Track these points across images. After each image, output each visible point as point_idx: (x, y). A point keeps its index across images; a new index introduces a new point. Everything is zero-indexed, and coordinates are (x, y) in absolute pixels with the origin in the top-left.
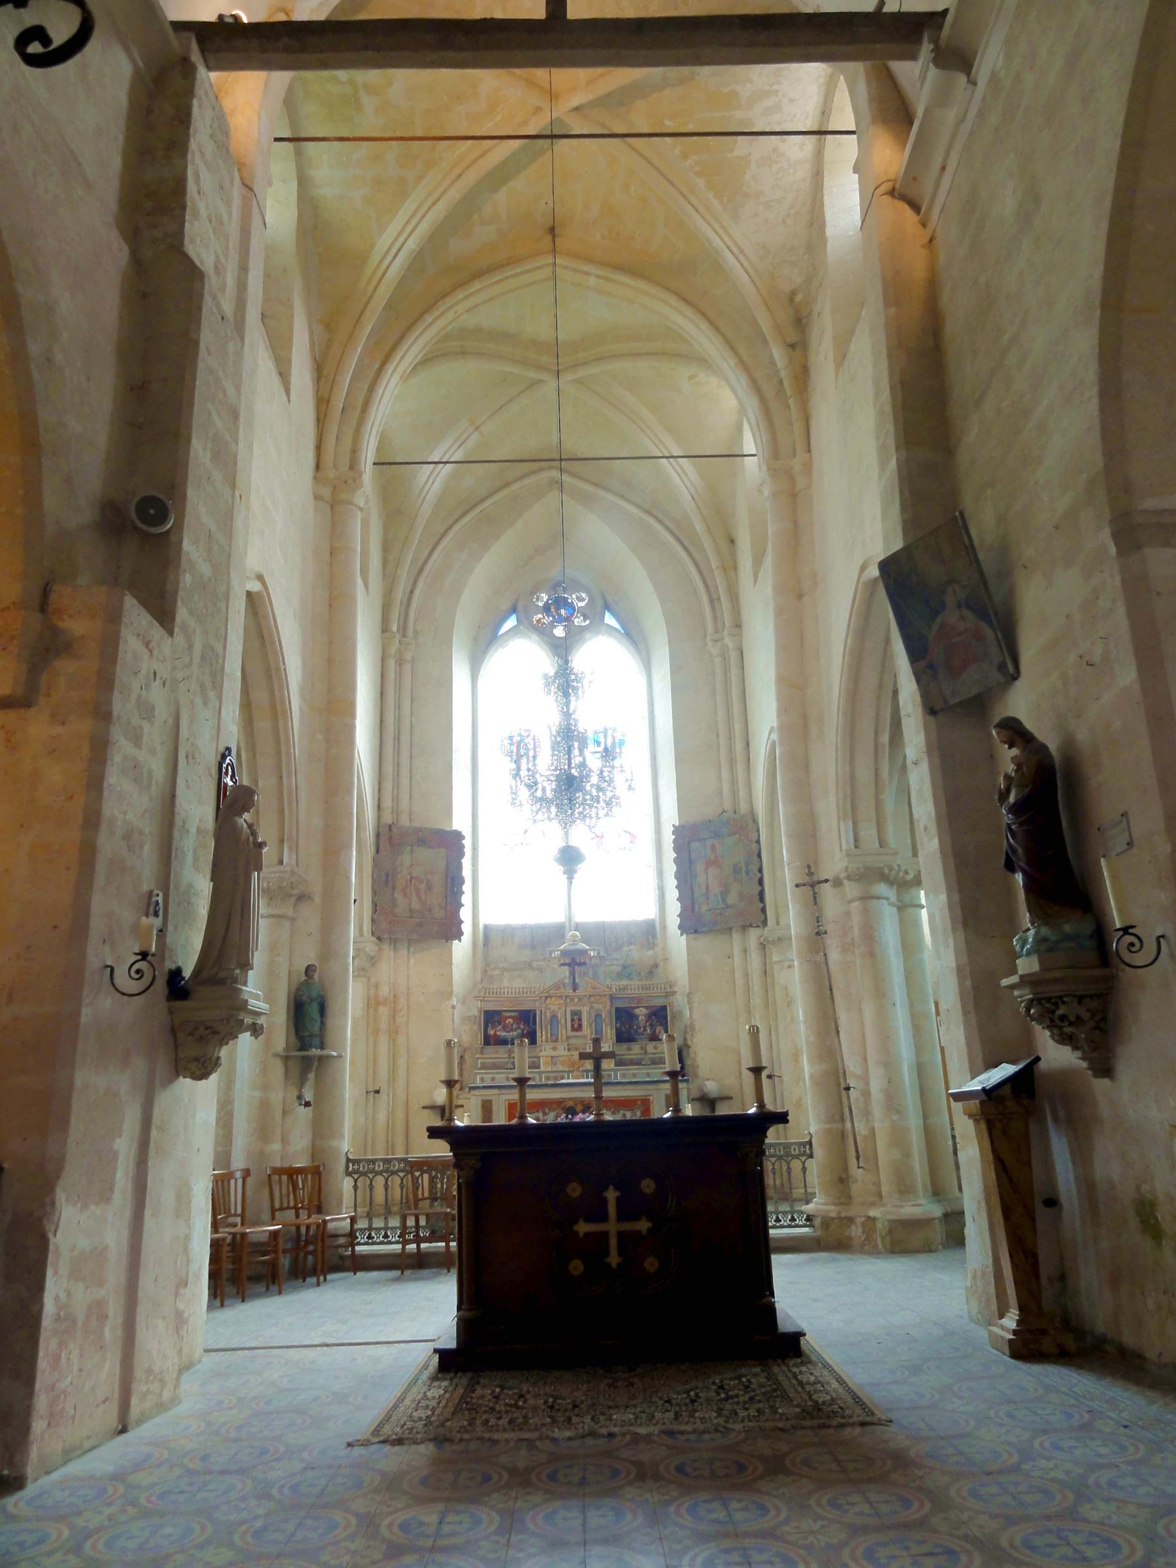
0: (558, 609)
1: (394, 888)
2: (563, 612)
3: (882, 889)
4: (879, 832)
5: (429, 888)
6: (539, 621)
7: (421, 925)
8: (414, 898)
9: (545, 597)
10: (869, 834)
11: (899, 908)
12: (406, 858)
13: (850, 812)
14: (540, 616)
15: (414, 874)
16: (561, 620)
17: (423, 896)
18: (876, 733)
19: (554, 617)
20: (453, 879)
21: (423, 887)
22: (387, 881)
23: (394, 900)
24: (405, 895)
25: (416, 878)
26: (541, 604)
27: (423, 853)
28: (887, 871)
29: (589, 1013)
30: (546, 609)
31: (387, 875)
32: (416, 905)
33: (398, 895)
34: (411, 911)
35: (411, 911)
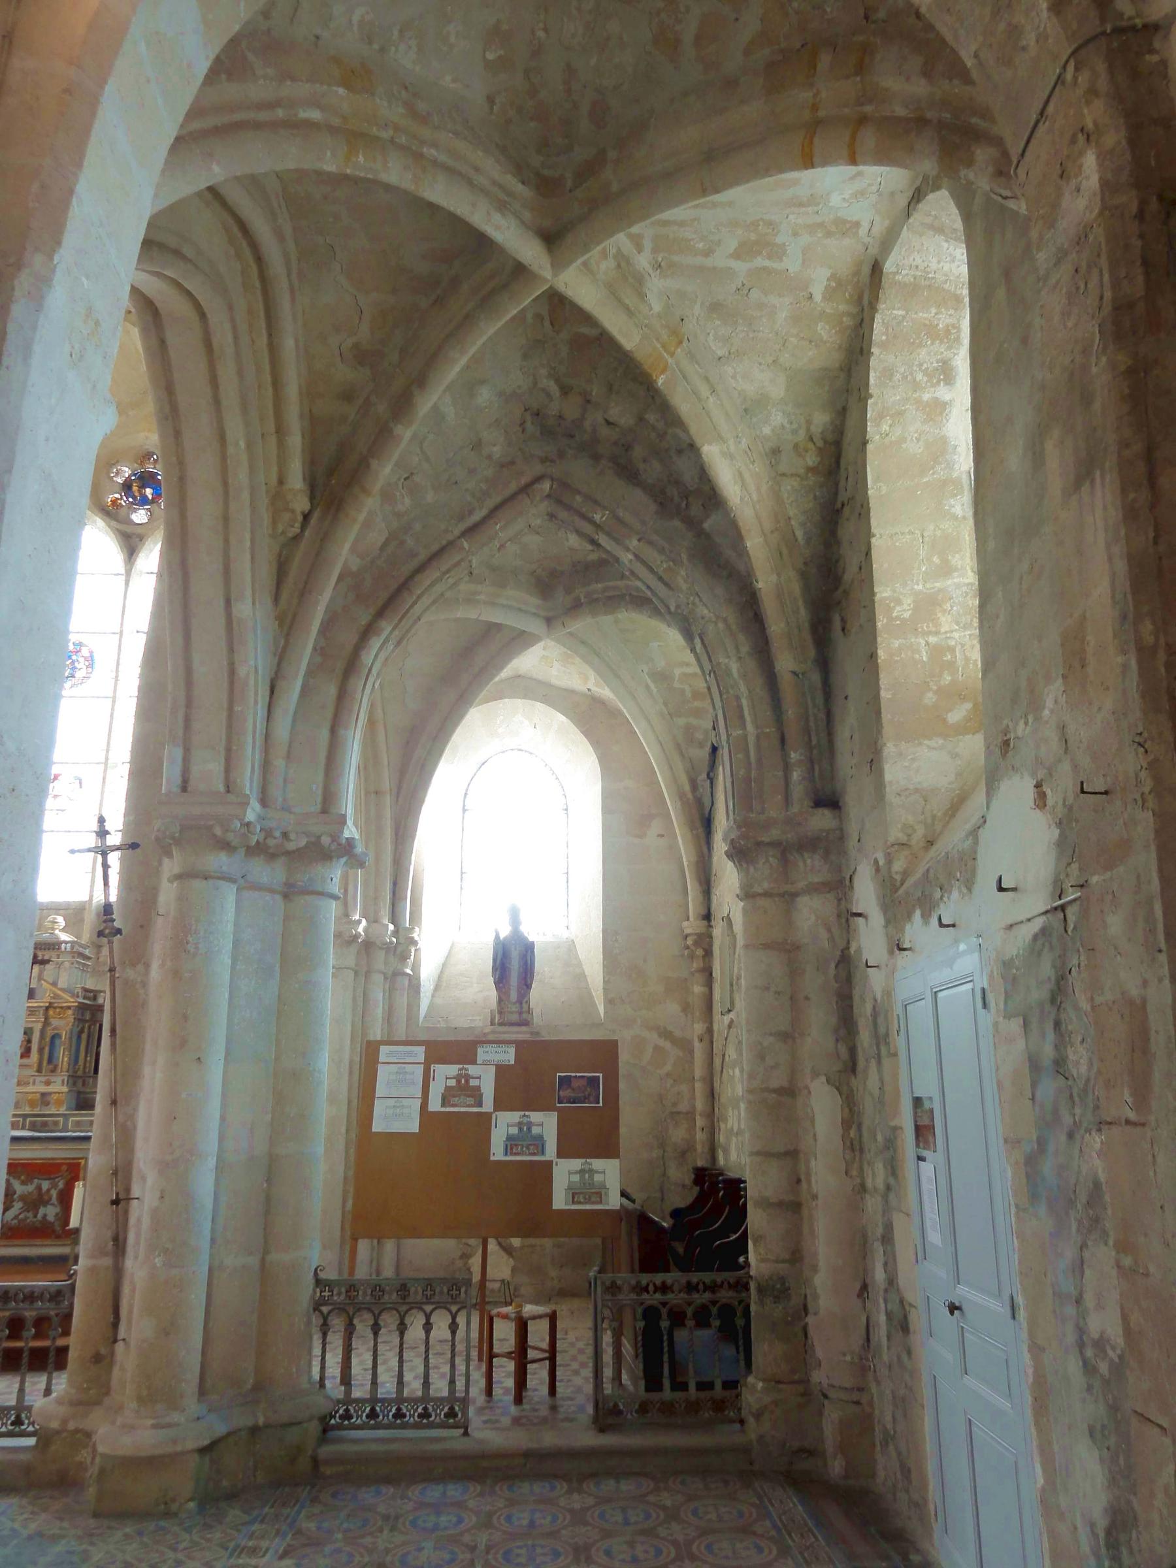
0: (143, 486)
2: (149, 492)
3: (220, 861)
4: (228, 770)
6: (114, 502)
9: (127, 472)
10: (208, 767)
11: (286, 896)
13: (180, 732)
14: (117, 496)
16: (144, 501)
18: (228, 602)
19: (134, 498)
26: (120, 480)
28: (218, 831)
29: (43, 1032)
30: (127, 487)
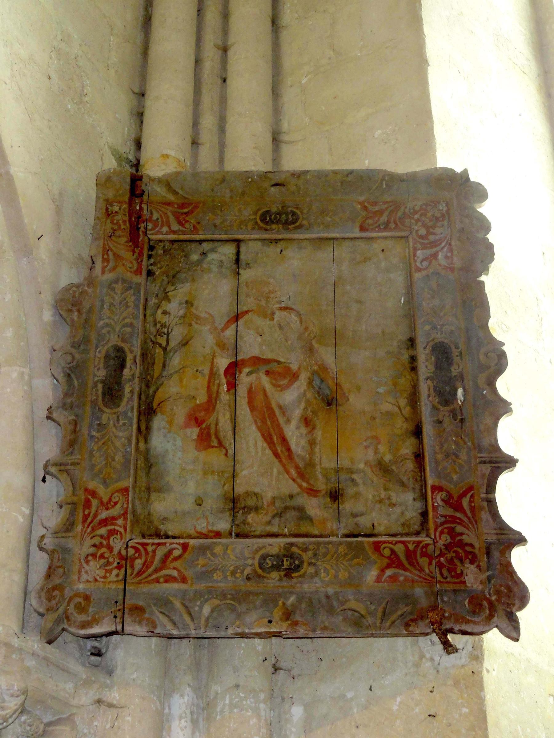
1: (148, 411)
5: (330, 401)
7: (289, 565)
8: (251, 444)
12: (212, 291)
15: (252, 346)
17: (295, 434)
20: (443, 354)
21: (292, 398)
22: (112, 393)
23: (148, 463)
24: (207, 438)
25: (257, 362)
27: (288, 270)
31: (118, 360)
32: (260, 474)
33: (171, 442)
34: (234, 504)
35: (234, 504)
